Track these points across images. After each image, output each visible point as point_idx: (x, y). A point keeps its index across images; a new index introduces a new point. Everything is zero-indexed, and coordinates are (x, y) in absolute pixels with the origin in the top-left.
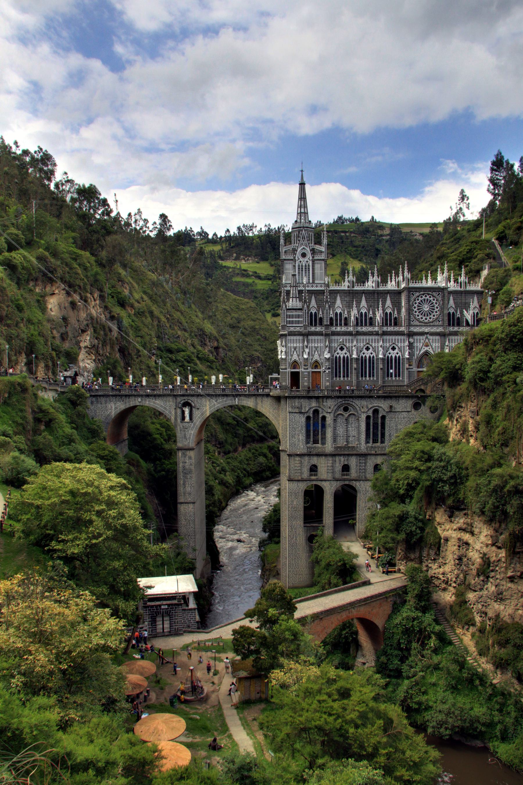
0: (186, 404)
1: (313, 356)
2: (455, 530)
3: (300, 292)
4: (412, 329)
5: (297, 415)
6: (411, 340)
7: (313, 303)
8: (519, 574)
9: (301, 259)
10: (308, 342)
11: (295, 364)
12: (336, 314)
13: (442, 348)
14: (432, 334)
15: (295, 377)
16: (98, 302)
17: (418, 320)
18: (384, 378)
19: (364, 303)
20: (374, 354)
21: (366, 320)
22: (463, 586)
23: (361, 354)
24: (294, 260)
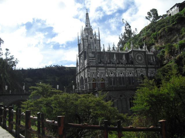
1: (101, 76)
4: (136, 66)
9: (90, 39)
14: (143, 68)
17: (137, 62)
24: (88, 39)
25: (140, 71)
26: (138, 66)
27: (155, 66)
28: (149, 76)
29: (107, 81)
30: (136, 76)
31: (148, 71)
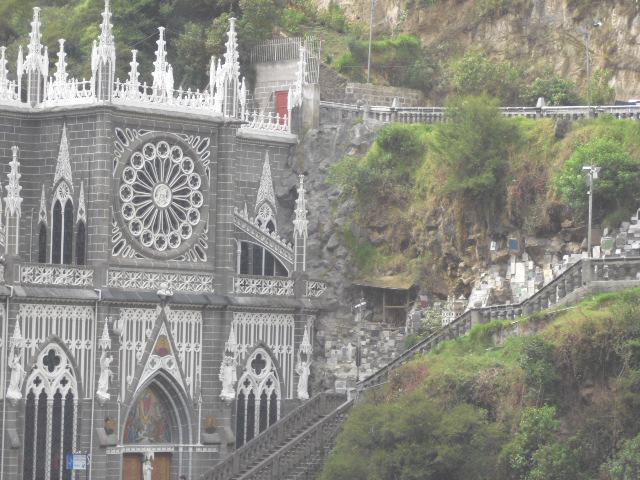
4: (114, 279)
13: (213, 359)
14: (177, 302)
17: (134, 243)
25: (147, 332)
26: (131, 283)
27: (299, 289)
28: (228, 394)
30: (104, 395)
31: (224, 337)
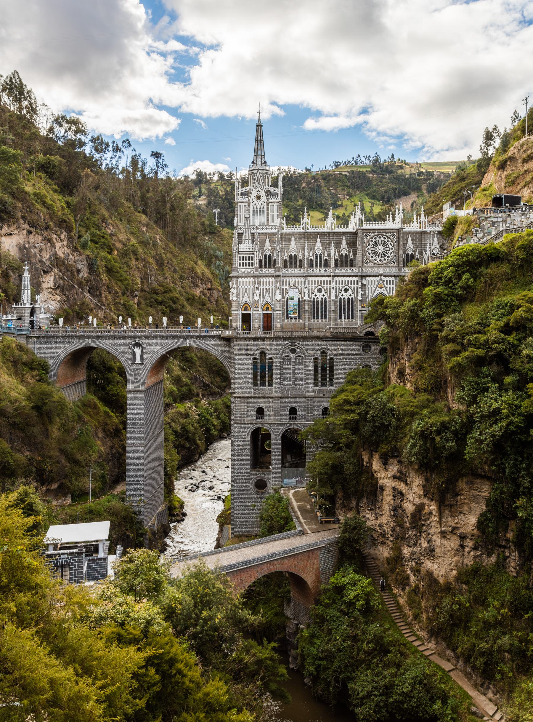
0: (138, 345)
1: (264, 298)
2: (390, 478)
3: (253, 234)
4: (365, 270)
5: (244, 356)
6: (364, 282)
7: (268, 245)
8: (450, 529)
10: (259, 284)
11: (246, 306)
12: (291, 256)
15: (246, 319)
16: (65, 243)
18: (336, 320)
19: (319, 244)
20: (326, 296)
21: (321, 261)
22: (401, 539)
23: (313, 296)
29: (278, 309)
